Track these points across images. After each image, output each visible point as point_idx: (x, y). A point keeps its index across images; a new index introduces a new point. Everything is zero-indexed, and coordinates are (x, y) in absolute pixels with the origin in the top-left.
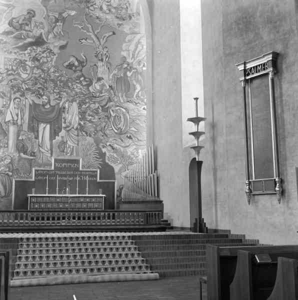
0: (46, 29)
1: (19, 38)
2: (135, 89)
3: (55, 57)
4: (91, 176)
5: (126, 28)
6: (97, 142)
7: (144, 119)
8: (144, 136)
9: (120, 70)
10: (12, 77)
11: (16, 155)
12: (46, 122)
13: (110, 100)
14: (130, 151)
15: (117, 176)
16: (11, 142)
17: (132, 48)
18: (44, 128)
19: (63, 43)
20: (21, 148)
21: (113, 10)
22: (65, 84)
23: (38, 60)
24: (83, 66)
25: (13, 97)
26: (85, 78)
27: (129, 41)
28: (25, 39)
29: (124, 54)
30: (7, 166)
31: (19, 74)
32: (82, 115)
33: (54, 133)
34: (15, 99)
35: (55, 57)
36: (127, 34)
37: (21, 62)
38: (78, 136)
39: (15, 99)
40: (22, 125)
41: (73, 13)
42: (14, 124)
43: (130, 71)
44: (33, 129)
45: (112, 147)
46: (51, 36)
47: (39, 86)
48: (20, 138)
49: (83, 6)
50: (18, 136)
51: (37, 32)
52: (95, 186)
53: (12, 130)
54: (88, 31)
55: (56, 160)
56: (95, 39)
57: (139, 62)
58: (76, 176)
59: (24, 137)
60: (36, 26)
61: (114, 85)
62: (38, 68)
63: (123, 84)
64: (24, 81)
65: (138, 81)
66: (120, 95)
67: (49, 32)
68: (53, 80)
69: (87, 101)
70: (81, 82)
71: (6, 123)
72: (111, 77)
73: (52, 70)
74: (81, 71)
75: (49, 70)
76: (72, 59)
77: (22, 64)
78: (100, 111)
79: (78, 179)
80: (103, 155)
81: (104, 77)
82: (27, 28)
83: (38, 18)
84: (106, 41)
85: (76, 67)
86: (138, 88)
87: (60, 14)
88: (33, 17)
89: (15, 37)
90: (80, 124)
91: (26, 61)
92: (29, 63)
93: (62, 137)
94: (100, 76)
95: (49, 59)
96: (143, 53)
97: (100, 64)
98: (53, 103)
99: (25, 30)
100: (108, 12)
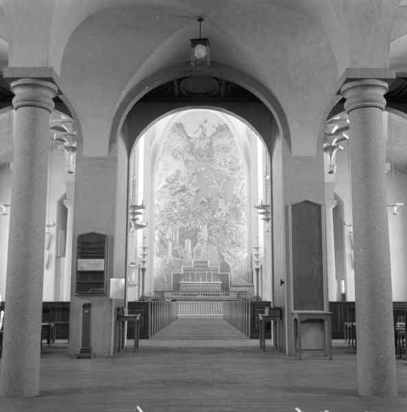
1: (172, 188)
2: (241, 215)
3: (192, 198)
5: (236, 176)
6: (219, 249)
7: (247, 233)
8: (246, 246)
11: (173, 259)
12: (188, 238)
14: (239, 254)
15: (232, 270)
16: (170, 252)
17: (240, 189)
18: (188, 242)
19: (198, 188)
20: (175, 254)
23: (183, 201)
27: (238, 184)
28: (175, 188)
30: (167, 265)
31: (173, 211)
32: (210, 233)
33: (194, 245)
41: (203, 169)
44: (182, 243)
46: (190, 185)
50: (173, 247)
51: (182, 184)
53: (170, 244)
55: (195, 262)
56: (217, 184)
58: (205, 270)
60: (181, 180)
61: (229, 214)
63: (235, 212)
64: (176, 215)
65: (243, 210)
67: (188, 184)
68: (192, 213)
75: (190, 206)
78: (220, 229)
79: (207, 272)
80: (222, 257)
82: (177, 182)
83: (183, 175)
86: (244, 214)
89: (169, 189)
90: (208, 238)
94: (220, 207)
97: (220, 200)
98: (192, 226)
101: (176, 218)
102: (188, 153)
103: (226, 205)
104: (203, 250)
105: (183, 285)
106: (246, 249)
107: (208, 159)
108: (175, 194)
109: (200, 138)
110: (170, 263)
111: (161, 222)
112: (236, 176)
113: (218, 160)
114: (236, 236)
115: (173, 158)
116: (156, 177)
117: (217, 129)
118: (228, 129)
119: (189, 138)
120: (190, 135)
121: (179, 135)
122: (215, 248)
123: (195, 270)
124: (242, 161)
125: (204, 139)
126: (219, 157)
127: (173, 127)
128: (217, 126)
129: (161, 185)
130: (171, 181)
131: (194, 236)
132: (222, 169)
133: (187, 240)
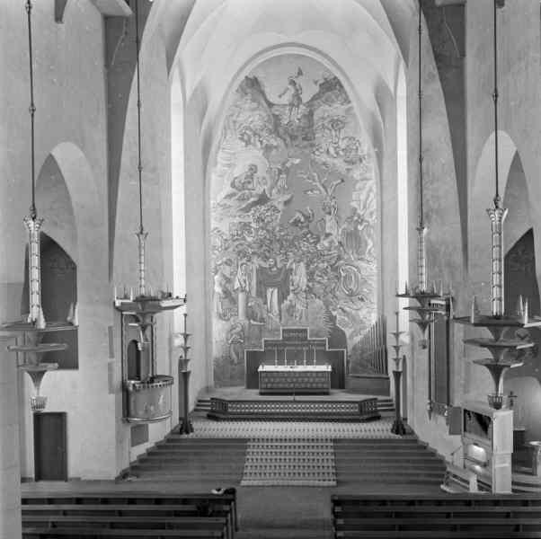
0: (269, 183)
1: (242, 199)
2: (366, 245)
3: (279, 215)
4: (318, 345)
5: (356, 174)
6: (327, 304)
7: (375, 278)
8: (375, 299)
9: (349, 223)
10: (237, 243)
13: (339, 258)
17: (363, 197)
19: (287, 197)
20: (250, 315)
21: (341, 153)
22: (292, 244)
23: (263, 221)
24: (310, 222)
25: (240, 263)
26: (312, 234)
27: (360, 189)
28: (248, 199)
29: (354, 204)
30: (238, 334)
31: (244, 239)
32: (311, 276)
33: (282, 298)
34: (242, 265)
35: (279, 215)
36: (357, 181)
37: (245, 225)
38: (306, 298)
39: (242, 265)
40: (250, 291)
41: (297, 161)
42: (242, 291)
43: (361, 224)
44: (261, 294)
45: (343, 310)
46: (274, 191)
47: (266, 247)
48: (249, 304)
49: (307, 151)
50: (247, 304)
51: (259, 190)
52: (324, 357)
53: (241, 297)
54: (314, 180)
55: (284, 330)
57: (371, 214)
59: (253, 303)
61: (344, 242)
62: (263, 229)
63: (353, 239)
65: (369, 236)
66: (351, 252)
67: (272, 188)
69: (315, 260)
70: (308, 239)
71: (234, 291)
72: (340, 232)
73: (278, 229)
74: (308, 227)
75: (274, 229)
76: (298, 215)
77: (246, 226)
78: (329, 270)
80: (332, 319)
81: (332, 232)
82: (250, 186)
83: (260, 173)
84: (334, 190)
85: (302, 223)
87: (284, 164)
88: (255, 172)
89: (238, 199)
90: (308, 286)
91: (250, 223)
92: (253, 225)
93: (291, 301)
94: (328, 231)
95: (273, 218)
96: (374, 206)
97: (328, 218)
99: (249, 189)
100: (335, 155)
101: (250, 251)
102: (271, 133)
103: (339, 226)
104: (298, 306)
105: (263, 375)
106: (376, 306)
107: (306, 143)
108: (247, 210)
109: (292, 105)
110: (242, 330)
111: (224, 259)
112: (356, 174)
113: (324, 146)
114: (357, 281)
115: (244, 144)
116: (214, 178)
117: (320, 85)
118: (341, 86)
119: (270, 105)
120: (271, 100)
121: (253, 100)
122: (319, 302)
123: (285, 345)
124: (366, 147)
125: (298, 106)
126: (324, 139)
127: (240, 86)
128: (322, 81)
129: (223, 194)
130: (241, 186)
131: (280, 281)
132: (329, 160)
133: (271, 290)
